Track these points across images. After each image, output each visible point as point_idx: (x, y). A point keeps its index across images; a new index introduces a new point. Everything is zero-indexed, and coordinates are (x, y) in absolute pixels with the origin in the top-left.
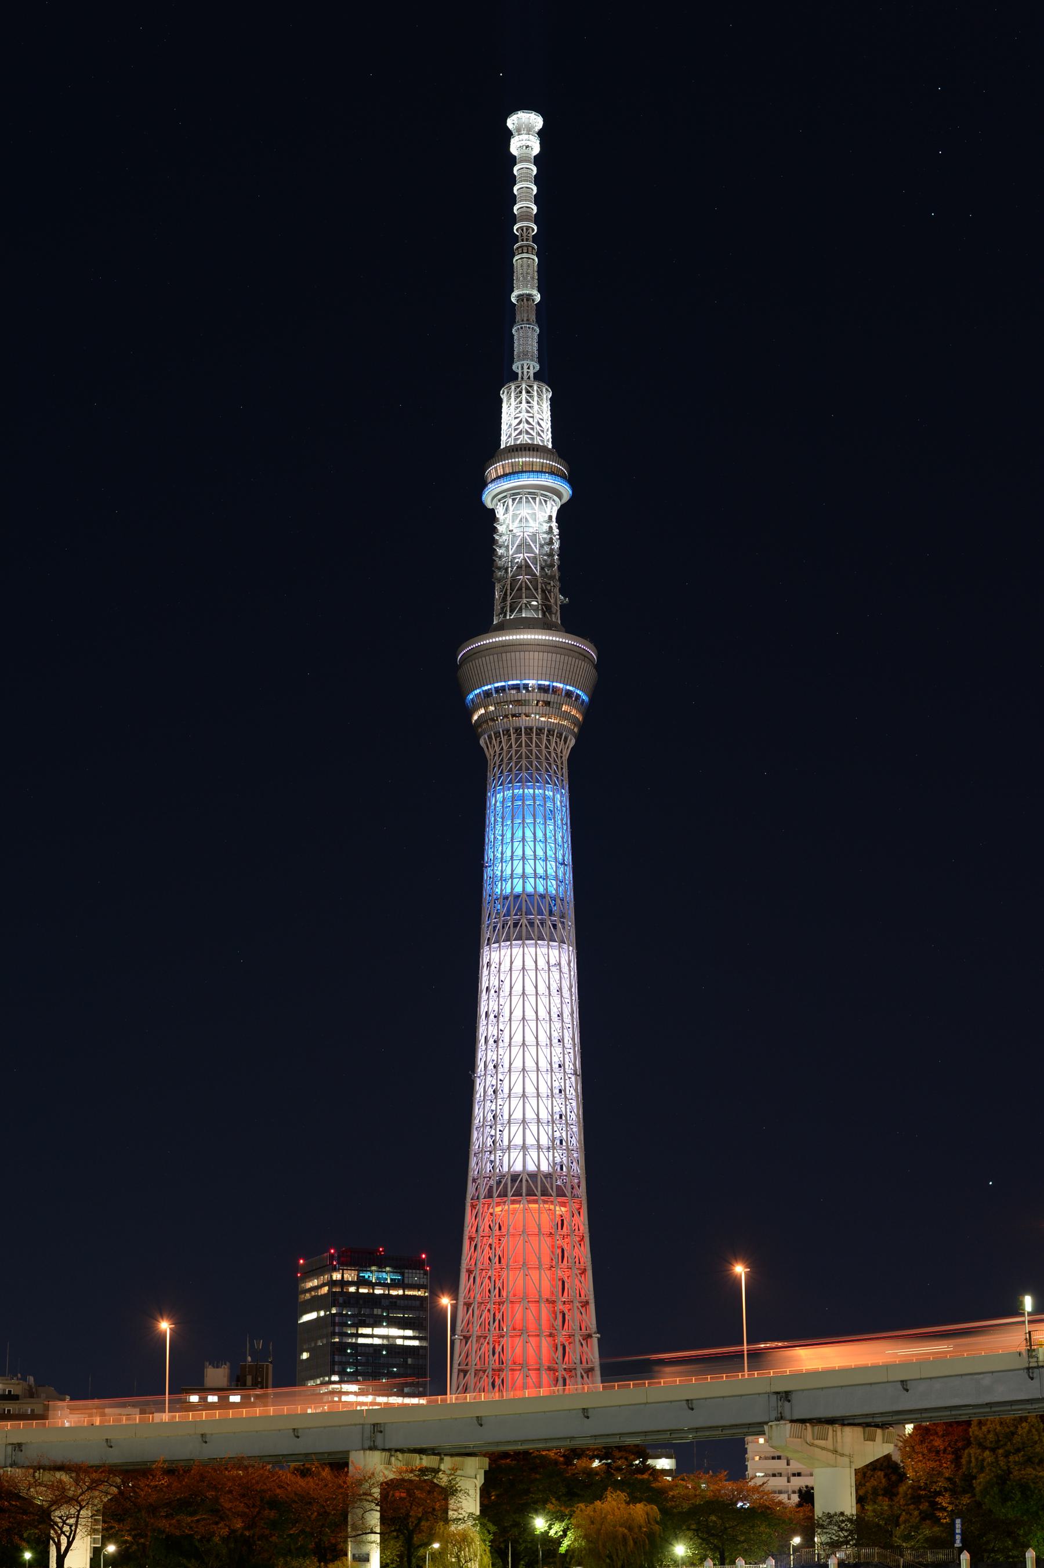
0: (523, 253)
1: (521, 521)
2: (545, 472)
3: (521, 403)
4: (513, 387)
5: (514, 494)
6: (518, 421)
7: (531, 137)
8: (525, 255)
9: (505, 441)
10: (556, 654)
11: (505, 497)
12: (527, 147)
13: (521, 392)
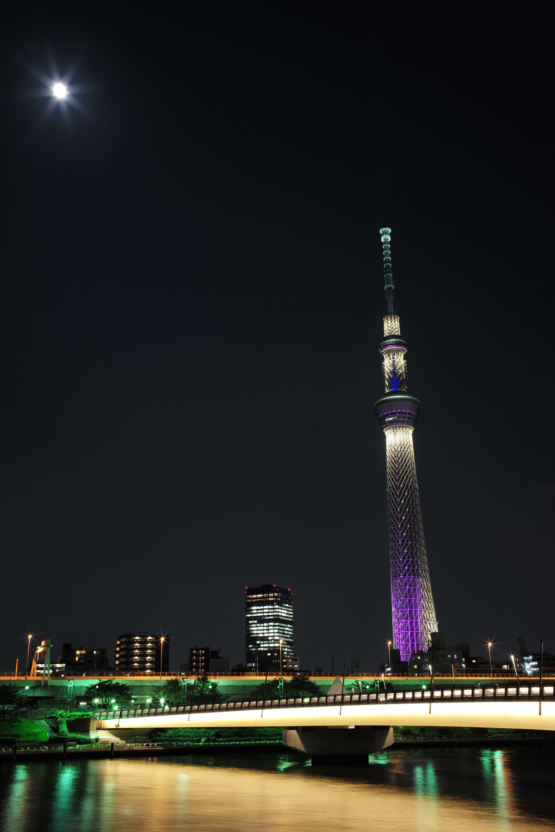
0: (387, 274)
1: (399, 359)
2: (401, 345)
3: (392, 321)
4: (389, 317)
5: (393, 351)
7: (389, 236)
8: (388, 274)
9: (386, 334)
10: (406, 401)
11: (390, 351)
12: (386, 239)
13: (392, 318)
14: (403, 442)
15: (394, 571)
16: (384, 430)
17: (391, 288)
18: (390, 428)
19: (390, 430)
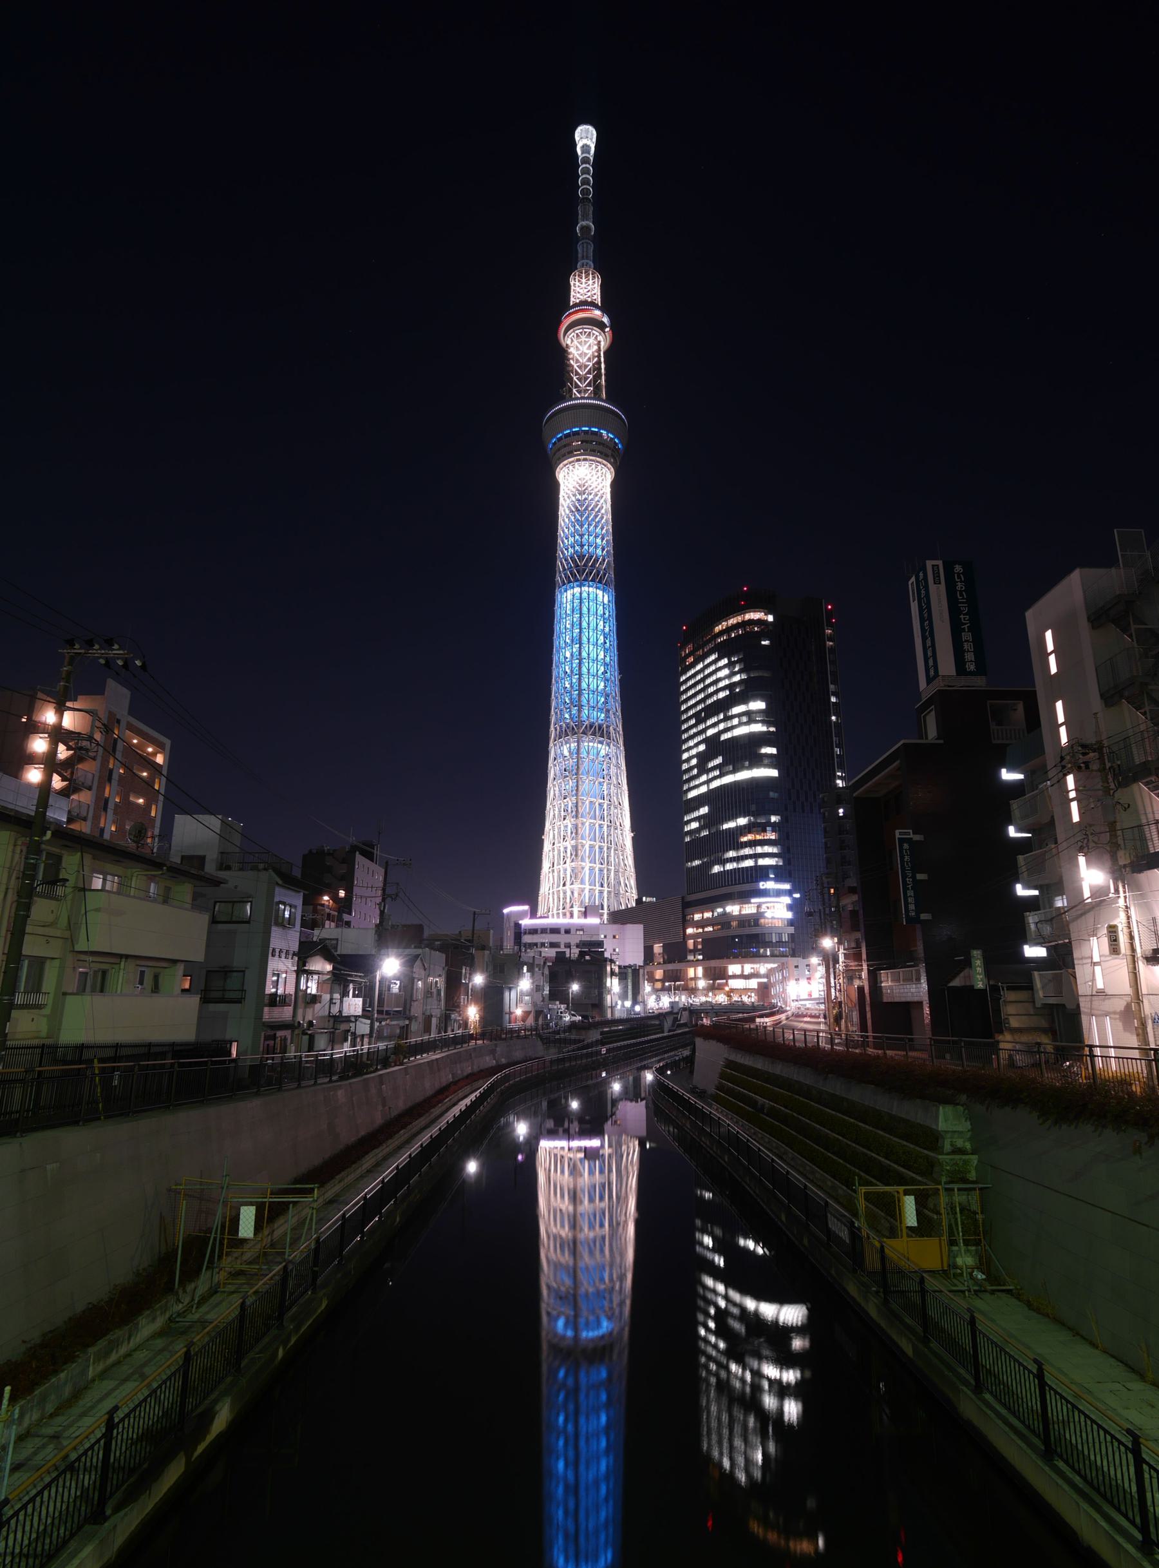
3: (589, 280)
6: (587, 290)
13: (589, 274)
14: (596, 490)
15: (561, 726)
16: (558, 470)
17: (588, 228)
18: (573, 462)
19: (571, 468)
